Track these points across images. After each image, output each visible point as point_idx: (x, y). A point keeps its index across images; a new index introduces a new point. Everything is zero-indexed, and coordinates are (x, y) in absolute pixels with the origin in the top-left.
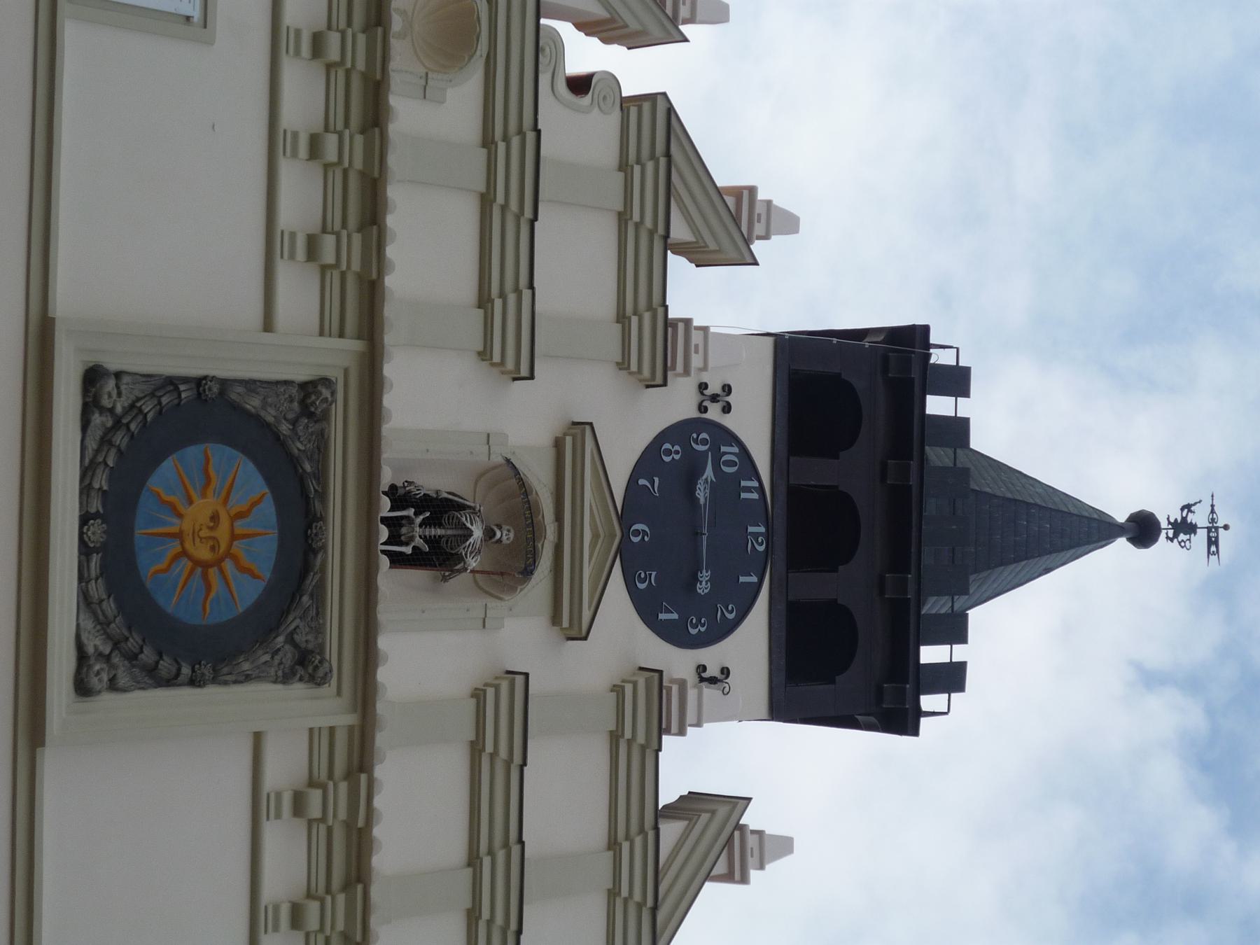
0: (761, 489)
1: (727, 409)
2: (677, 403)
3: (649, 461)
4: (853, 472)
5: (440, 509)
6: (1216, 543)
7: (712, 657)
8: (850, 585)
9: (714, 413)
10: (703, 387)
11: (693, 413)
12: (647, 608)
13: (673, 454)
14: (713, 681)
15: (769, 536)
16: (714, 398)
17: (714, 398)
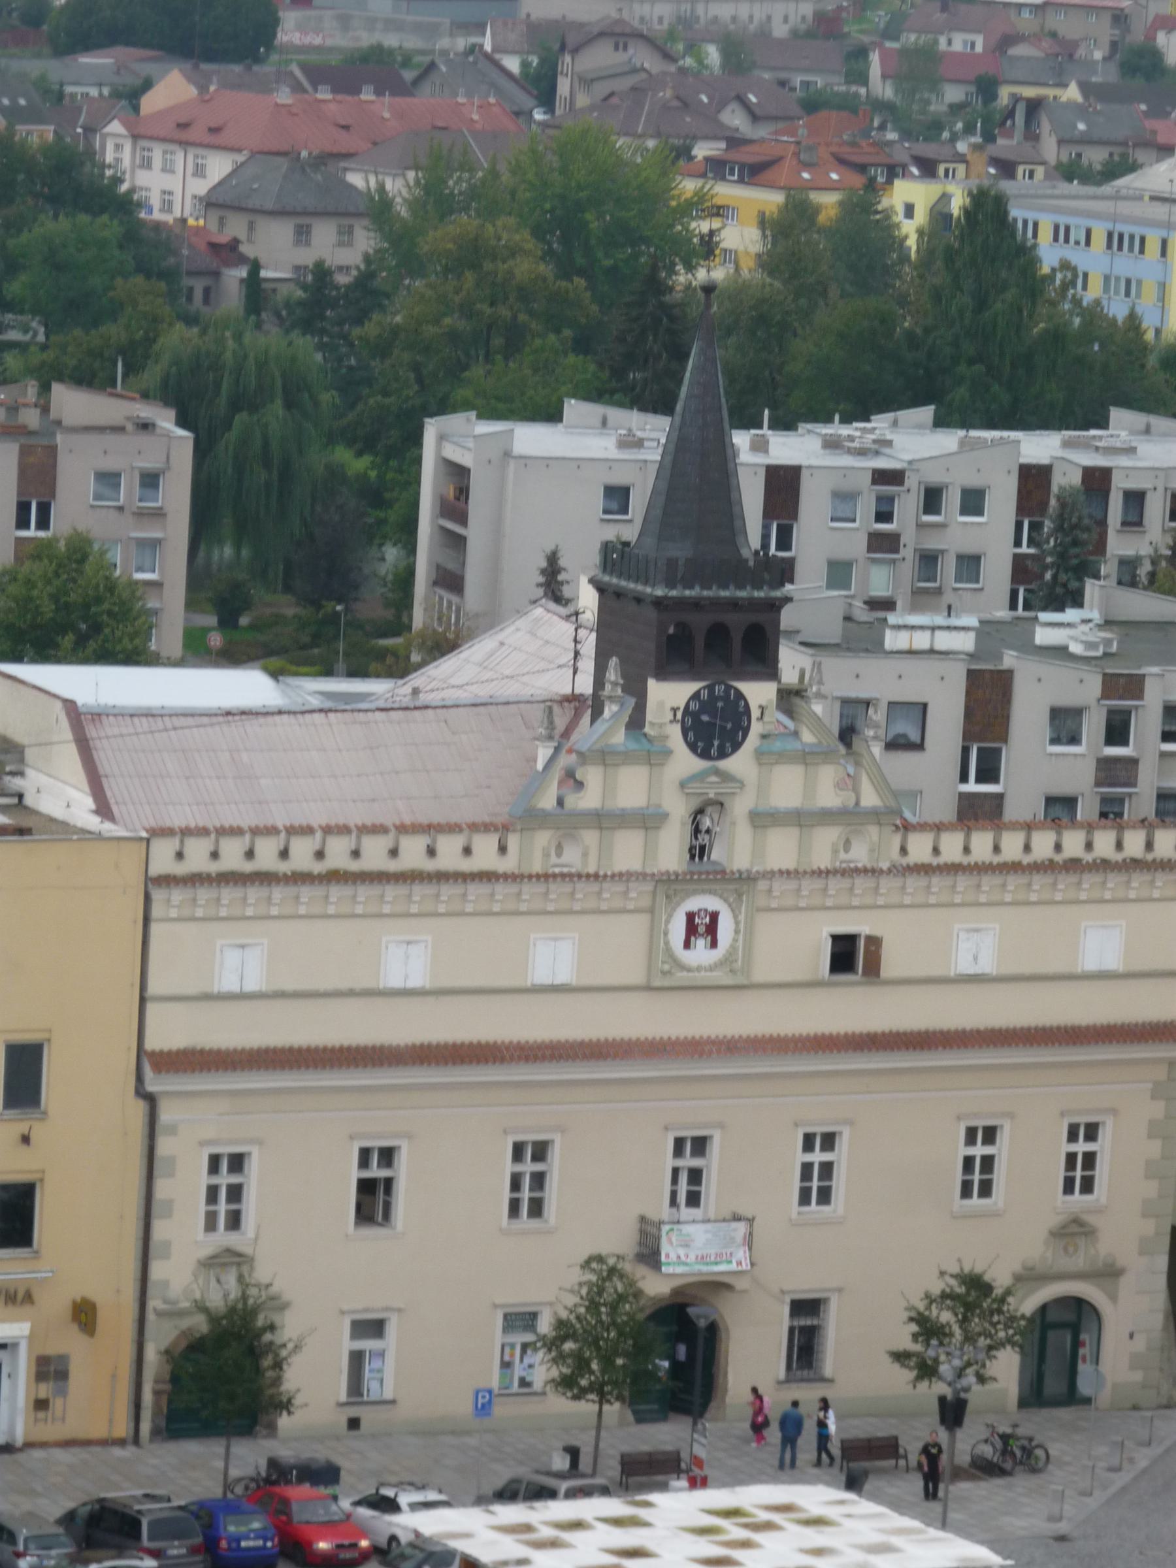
0: (704, 688)
1: (678, 708)
2: (675, 731)
3: (692, 747)
4: (700, 623)
5: (697, 831)
6: (719, 207)
7: (755, 713)
8: (737, 622)
9: (679, 715)
10: (671, 722)
11: (679, 726)
12: (737, 746)
13: (691, 735)
14: (762, 714)
15: (720, 684)
16: (675, 715)
17: (675, 715)
